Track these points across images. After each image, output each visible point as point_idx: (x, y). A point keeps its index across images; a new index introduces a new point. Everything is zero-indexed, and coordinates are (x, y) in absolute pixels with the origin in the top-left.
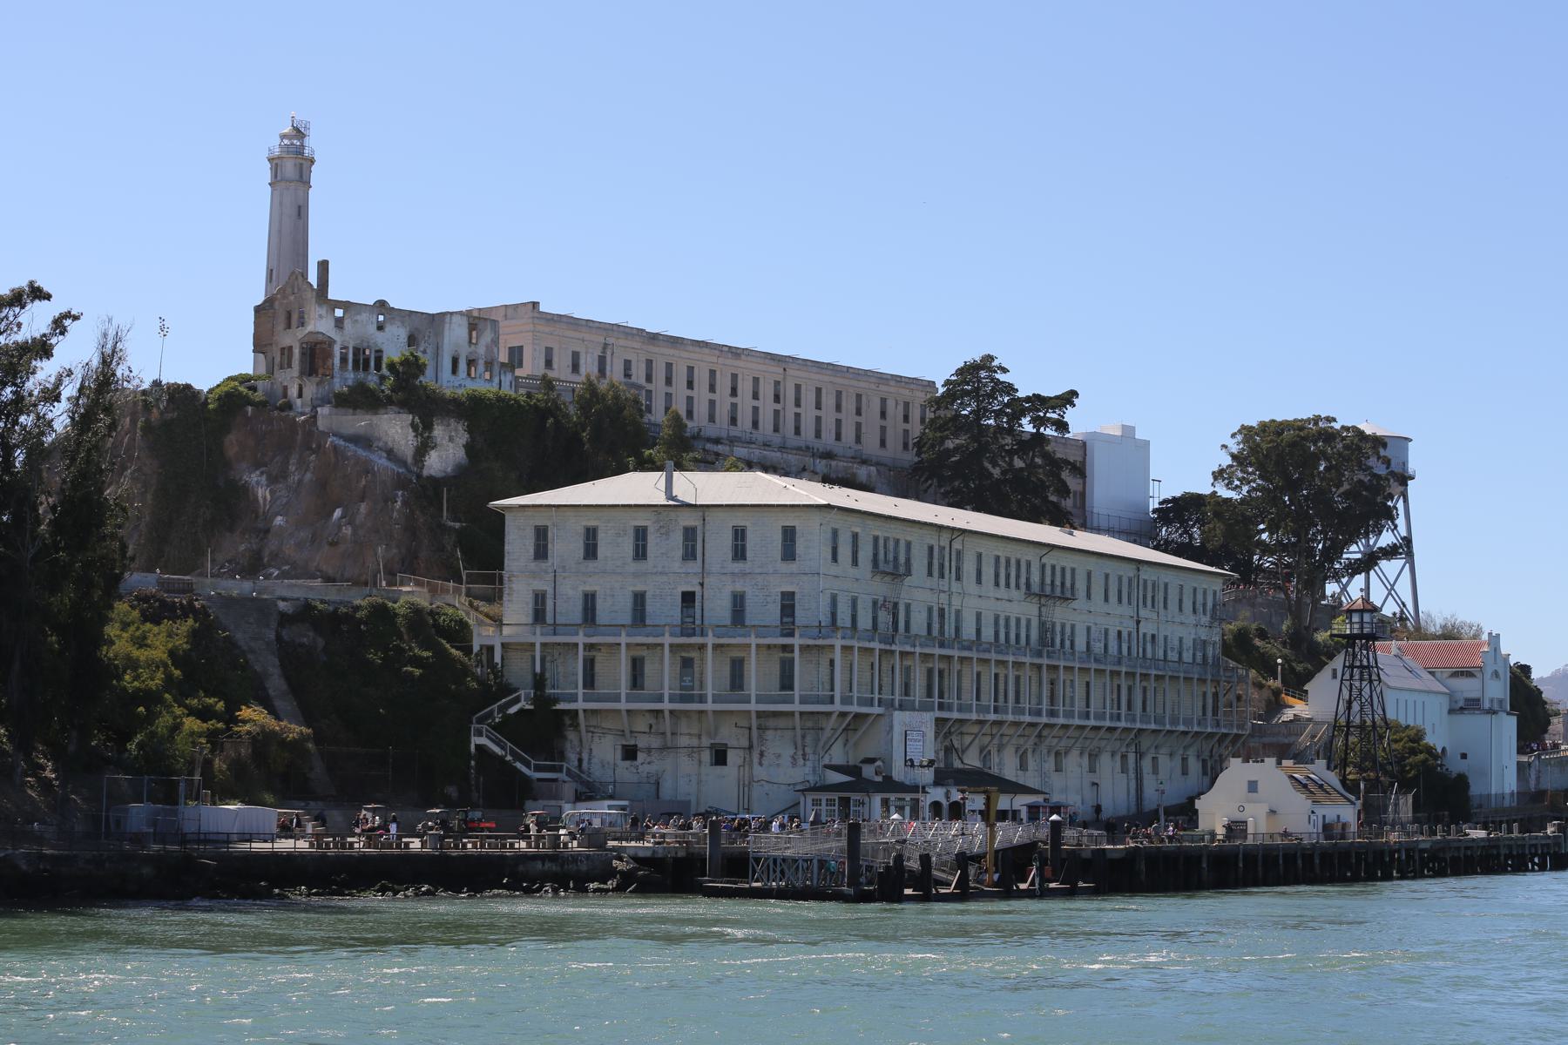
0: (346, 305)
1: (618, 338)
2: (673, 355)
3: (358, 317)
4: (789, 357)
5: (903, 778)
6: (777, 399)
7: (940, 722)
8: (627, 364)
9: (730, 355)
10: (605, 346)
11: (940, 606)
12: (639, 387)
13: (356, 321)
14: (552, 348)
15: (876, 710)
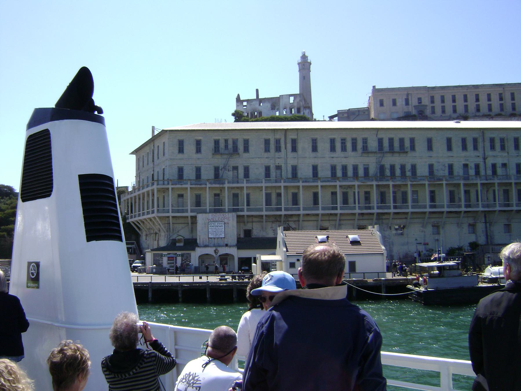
0: (248, 101)
1: (413, 91)
2: (444, 93)
3: (252, 103)
4: (506, 84)
5: (207, 244)
6: (501, 99)
7: (238, 216)
8: (420, 99)
9: (473, 88)
10: (408, 95)
11: (278, 165)
12: (426, 106)
13: (251, 105)
14: (383, 100)
15: (189, 214)
